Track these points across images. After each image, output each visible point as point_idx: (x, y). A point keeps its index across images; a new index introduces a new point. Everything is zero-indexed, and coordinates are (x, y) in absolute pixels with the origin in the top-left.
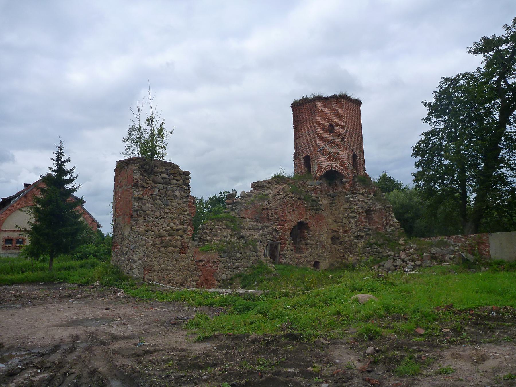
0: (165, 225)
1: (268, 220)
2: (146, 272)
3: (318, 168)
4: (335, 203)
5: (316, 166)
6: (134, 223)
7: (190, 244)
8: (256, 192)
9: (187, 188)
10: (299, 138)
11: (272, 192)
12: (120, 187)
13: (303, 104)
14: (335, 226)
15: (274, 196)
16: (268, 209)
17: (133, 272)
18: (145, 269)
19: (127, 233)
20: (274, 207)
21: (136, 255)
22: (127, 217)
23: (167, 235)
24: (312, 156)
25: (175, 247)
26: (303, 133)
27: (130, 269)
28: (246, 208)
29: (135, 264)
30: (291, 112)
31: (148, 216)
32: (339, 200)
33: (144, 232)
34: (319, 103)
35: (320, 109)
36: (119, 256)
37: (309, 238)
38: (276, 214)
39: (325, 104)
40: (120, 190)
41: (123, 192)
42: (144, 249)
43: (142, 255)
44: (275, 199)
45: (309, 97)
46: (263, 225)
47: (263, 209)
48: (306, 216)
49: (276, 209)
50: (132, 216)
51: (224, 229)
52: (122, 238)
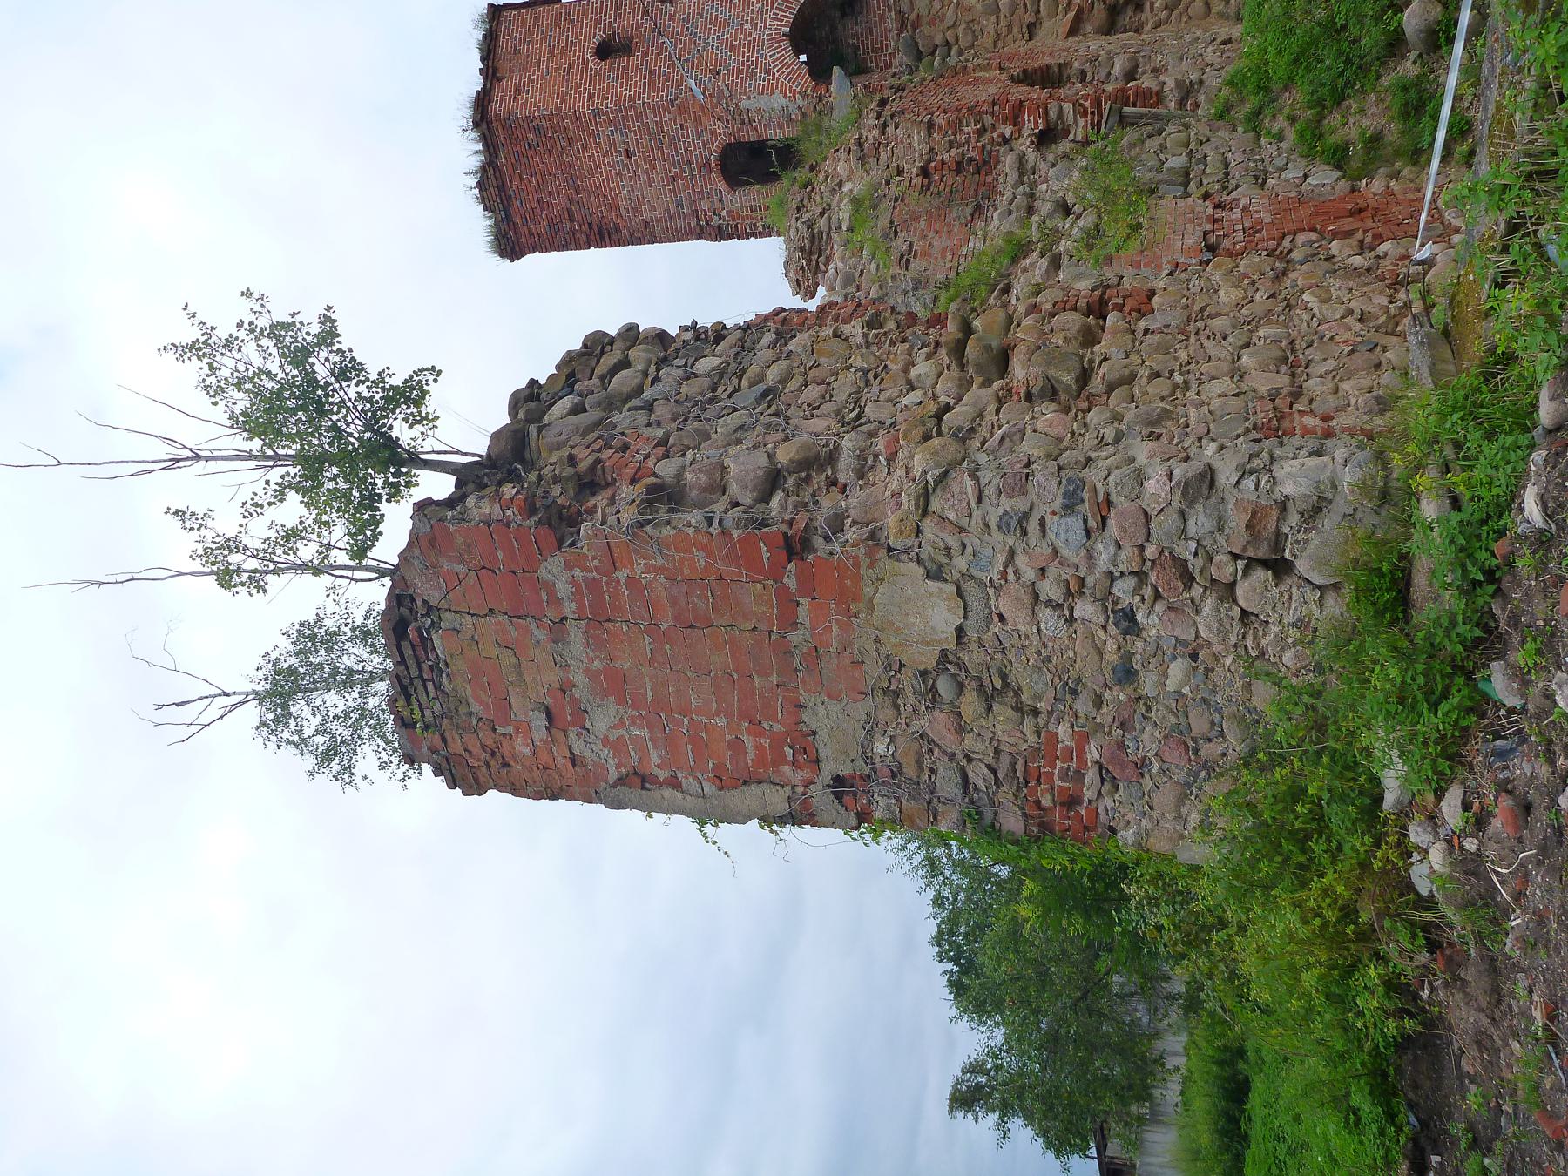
0: (913, 398)
1: (986, 164)
2: (1308, 421)
3: (775, 93)
4: (947, 44)
5: (763, 102)
6: (851, 534)
7: (1083, 286)
8: (837, 262)
9: (688, 336)
10: (646, 214)
11: (847, 187)
12: (580, 714)
13: (502, 188)
14: (1053, 29)
15: (862, 160)
16: (925, 172)
17: (1314, 512)
18: (1276, 430)
19: (935, 616)
20: (917, 139)
21: (1140, 478)
22: (804, 613)
23: (997, 385)
24: (722, 135)
25: (1090, 338)
26: (623, 192)
27: (1280, 567)
28: (904, 261)
29: (1226, 476)
30: (534, 262)
31: (818, 461)
32: (932, 23)
33: (936, 442)
34: (501, 105)
35: (529, 98)
36: (1148, 741)
37: (1103, 74)
38: (957, 126)
39: (511, 80)
40: (603, 720)
41: (615, 685)
42: (1089, 440)
43: (1142, 451)
44: (877, 147)
45: (475, 161)
46: (1013, 176)
47: (924, 189)
48: (987, 68)
49: (931, 125)
50: (795, 547)
51: (1007, 290)
52: (988, 697)
